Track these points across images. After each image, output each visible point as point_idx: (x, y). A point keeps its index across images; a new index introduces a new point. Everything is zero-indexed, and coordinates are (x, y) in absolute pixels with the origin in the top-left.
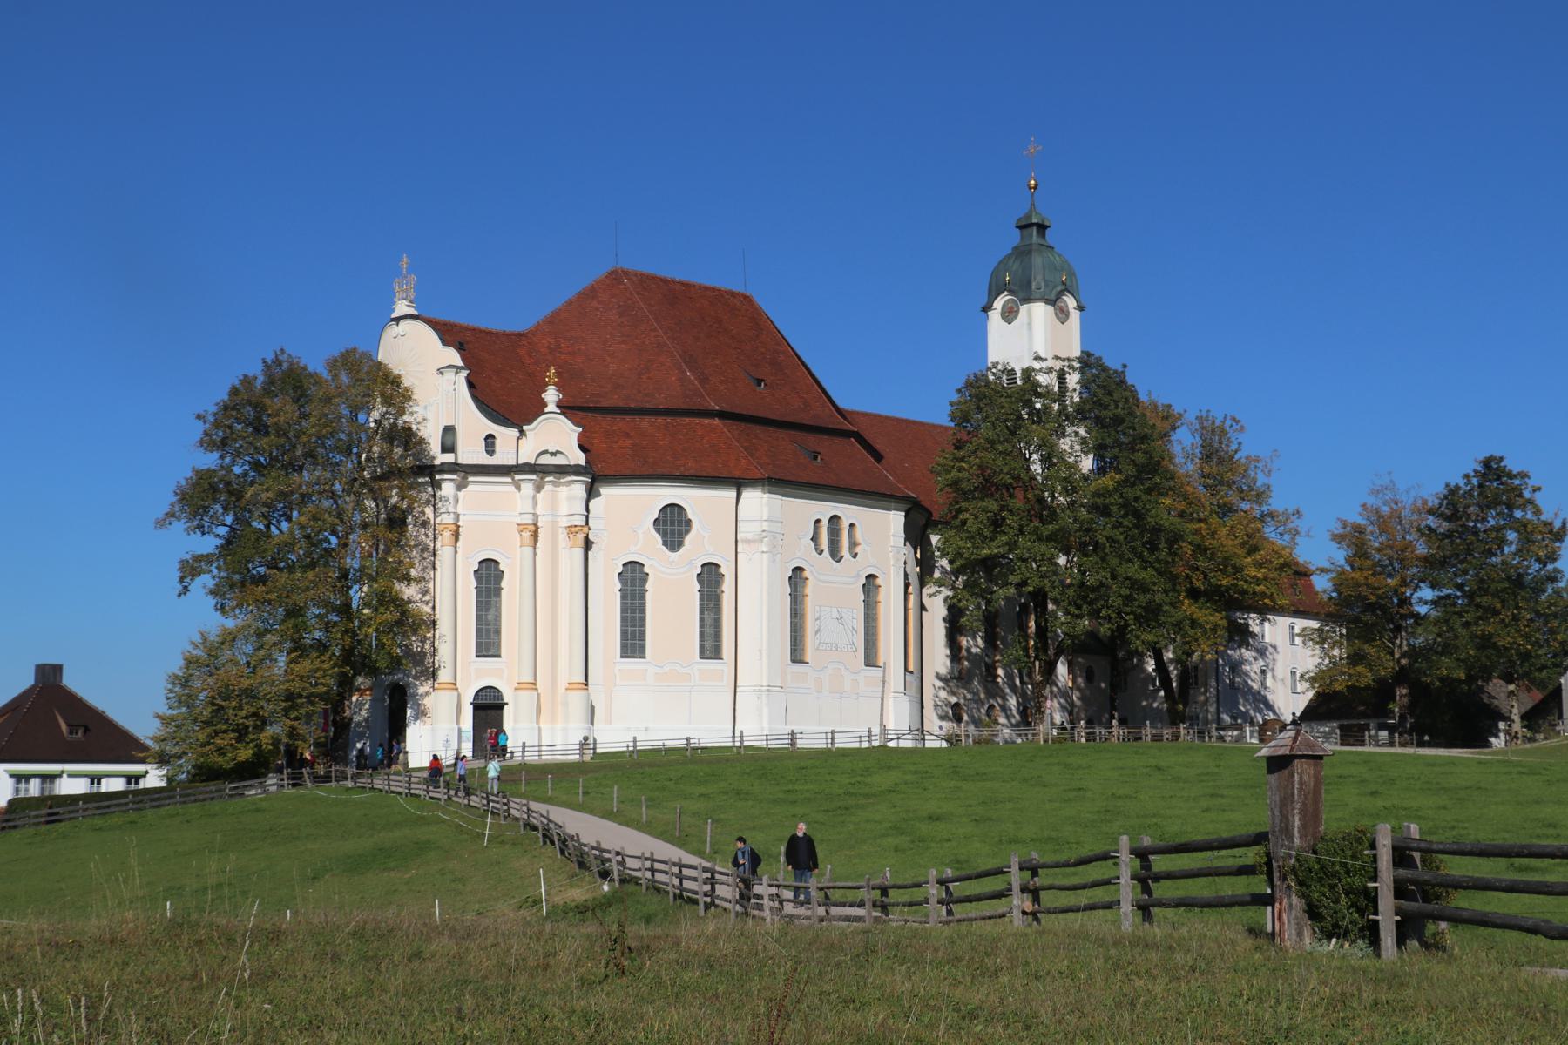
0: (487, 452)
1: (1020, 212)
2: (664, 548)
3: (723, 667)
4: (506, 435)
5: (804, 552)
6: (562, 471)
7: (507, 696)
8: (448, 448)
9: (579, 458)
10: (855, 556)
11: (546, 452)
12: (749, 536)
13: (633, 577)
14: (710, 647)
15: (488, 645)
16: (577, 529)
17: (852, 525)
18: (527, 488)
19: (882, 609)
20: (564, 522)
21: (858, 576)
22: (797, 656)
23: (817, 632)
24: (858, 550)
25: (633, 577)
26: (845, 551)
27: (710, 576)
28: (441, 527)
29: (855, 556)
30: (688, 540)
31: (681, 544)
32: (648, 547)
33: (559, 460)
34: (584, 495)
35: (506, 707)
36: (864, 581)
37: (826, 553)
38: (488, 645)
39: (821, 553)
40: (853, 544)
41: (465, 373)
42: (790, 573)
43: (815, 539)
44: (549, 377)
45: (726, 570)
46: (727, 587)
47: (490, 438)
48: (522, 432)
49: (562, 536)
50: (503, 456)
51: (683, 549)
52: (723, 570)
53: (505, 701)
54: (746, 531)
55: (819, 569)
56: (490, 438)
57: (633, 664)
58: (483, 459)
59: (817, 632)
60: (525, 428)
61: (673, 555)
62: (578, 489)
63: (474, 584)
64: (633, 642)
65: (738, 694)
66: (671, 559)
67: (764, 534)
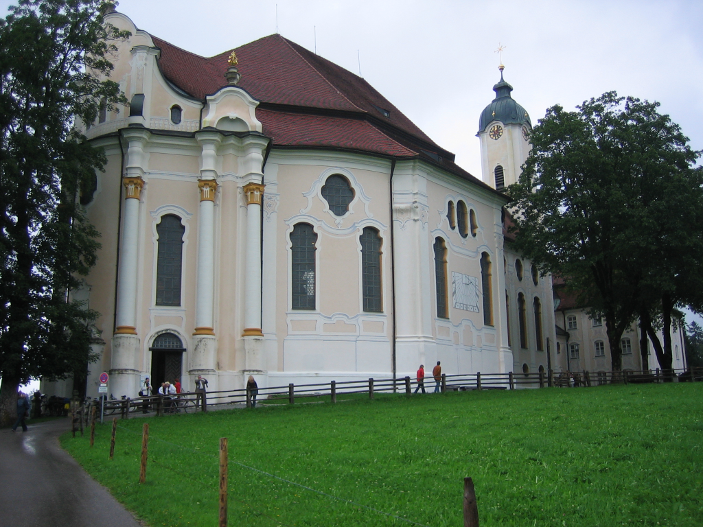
0: (172, 120)
1: (497, 81)
2: (331, 212)
3: (384, 319)
4: (189, 107)
5: (442, 227)
6: (241, 136)
7: (187, 341)
8: (136, 110)
9: (255, 124)
10: (474, 235)
11: (226, 119)
12: (402, 206)
13: (303, 236)
14: (372, 302)
15: (169, 292)
16: (254, 187)
17: (471, 211)
18: (209, 151)
19: (492, 278)
20: (242, 183)
21: (477, 252)
22: (442, 312)
23: (454, 293)
24: (477, 231)
25: (303, 236)
26: (469, 231)
27: (370, 237)
28: (127, 181)
29: (474, 235)
30: (351, 206)
31: (345, 210)
32: (316, 210)
33: (238, 128)
34: (261, 158)
35: (184, 353)
36: (481, 257)
37: (457, 228)
38: (169, 292)
39: (453, 228)
40: (473, 227)
41: (157, 52)
42: (434, 242)
43: (450, 216)
44: (231, 59)
45: (384, 234)
46: (385, 248)
47: (176, 109)
48: (205, 103)
49: (239, 196)
50: (188, 124)
51: (347, 213)
52: (381, 234)
53: (184, 347)
54: (400, 202)
55: (452, 239)
56: (176, 109)
57: (303, 316)
58: (168, 125)
59: (454, 293)
60: (208, 98)
61: (339, 219)
62: (257, 155)
63: (157, 237)
64: (303, 299)
65: (397, 344)
66: (337, 222)
67: (415, 205)
